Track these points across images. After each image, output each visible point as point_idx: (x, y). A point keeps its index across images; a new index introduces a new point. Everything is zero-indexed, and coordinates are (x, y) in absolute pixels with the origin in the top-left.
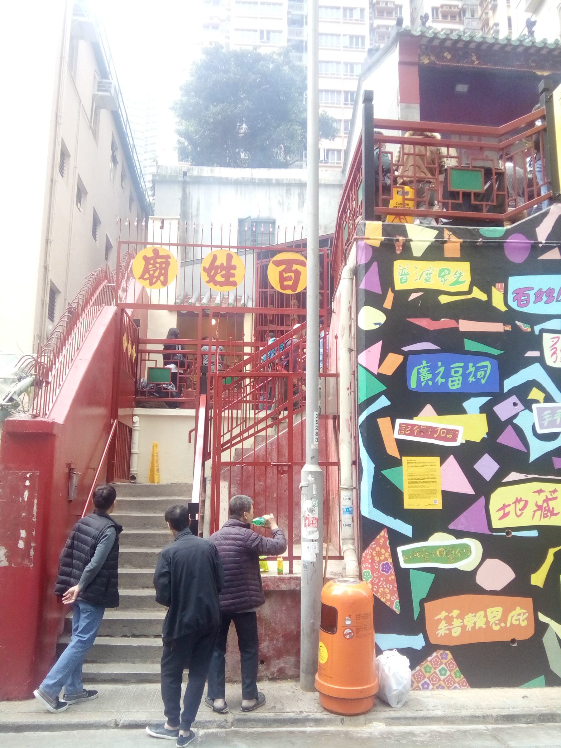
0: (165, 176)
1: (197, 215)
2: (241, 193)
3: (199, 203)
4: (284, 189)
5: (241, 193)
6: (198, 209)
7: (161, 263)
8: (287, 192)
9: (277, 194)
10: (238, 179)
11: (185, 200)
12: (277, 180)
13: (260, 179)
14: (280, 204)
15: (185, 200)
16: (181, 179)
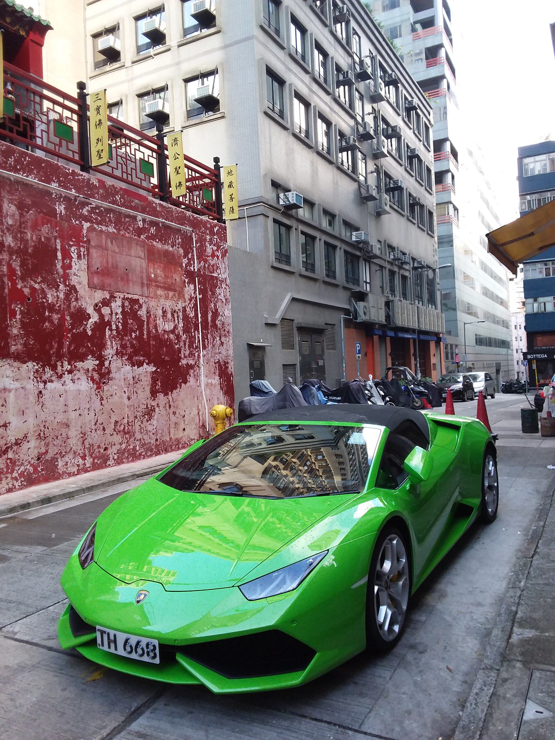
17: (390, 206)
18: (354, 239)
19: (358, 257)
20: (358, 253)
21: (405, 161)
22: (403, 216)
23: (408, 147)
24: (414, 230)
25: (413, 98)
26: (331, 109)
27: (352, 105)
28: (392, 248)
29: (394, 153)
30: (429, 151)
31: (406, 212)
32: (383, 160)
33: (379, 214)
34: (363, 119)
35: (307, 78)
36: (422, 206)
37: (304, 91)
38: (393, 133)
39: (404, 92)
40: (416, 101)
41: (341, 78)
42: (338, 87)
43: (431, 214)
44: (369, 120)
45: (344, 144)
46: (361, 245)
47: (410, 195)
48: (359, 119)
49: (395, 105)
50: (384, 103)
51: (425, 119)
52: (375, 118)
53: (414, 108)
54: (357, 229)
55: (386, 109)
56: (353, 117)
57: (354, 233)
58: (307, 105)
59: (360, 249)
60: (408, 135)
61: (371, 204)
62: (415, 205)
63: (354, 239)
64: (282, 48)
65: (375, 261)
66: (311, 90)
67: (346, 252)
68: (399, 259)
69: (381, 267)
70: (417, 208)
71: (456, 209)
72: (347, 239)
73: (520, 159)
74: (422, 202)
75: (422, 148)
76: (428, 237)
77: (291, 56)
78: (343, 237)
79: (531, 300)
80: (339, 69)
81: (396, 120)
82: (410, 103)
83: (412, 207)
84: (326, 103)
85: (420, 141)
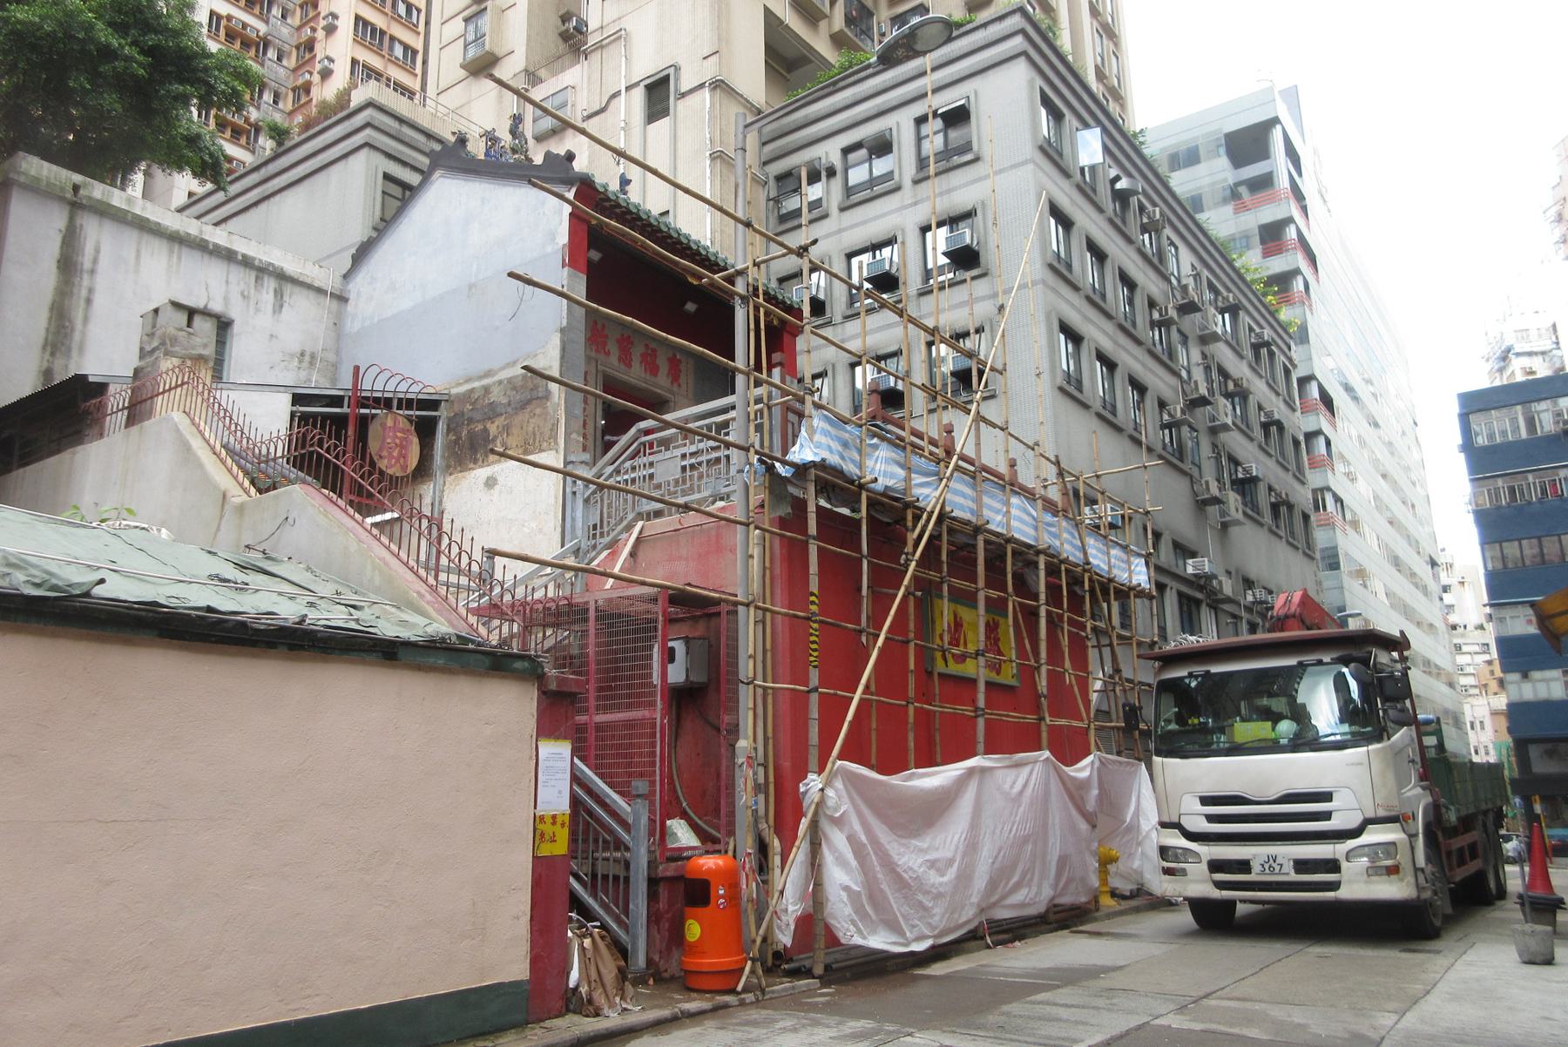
0: (38, 179)
1: (92, 272)
2: (179, 258)
3: (97, 251)
4: (253, 274)
5: (179, 258)
6: (95, 261)
7: (402, 439)
8: (257, 278)
9: (240, 279)
10: (177, 232)
11: (71, 239)
12: (244, 256)
13: (216, 245)
14: (244, 296)
15: (71, 239)
16: (69, 195)
17: (1245, 513)
18: (1190, 570)
19: (1198, 603)
20: (1199, 595)
21: (1258, 433)
22: (1261, 525)
23: (1260, 408)
24: (1281, 548)
25: (1261, 327)
26: (1143, 365)
27: (1171, 354)
28: (1249, 583)
29: (1239, 422)
30: (1294, 410)
31: (1267, 518)
32: (1223, 436)
33: (1225, 526)
34: (1189, 372)
35: (1109, 327)
36: (1290, 507)
37: (1107, 346)
38: (1240, 395)
39: (1247, 319)
40: (1267, 334)
41: (1156, 316)
42: (1152, 329)
43: (1306, 517)
44: (1198, 374)
45: (1166, 417)
46: (1202, 582)
47: (1270, 489)
48: (1184, 374)
49: (1234, 343)
50: (1221, 346)
51: (1283, 358)
52: (1207, 369)
53: (1267, 344)
54: (1193, 555)
55: (1223, 353)
56: (1176, 374)
57: (1190, 561)
58: (1110, 365)
59: (1201, 588)
60: (1259, 389)
61: (1213, 510)
62: (1281, 506)
63: (1190, 570)
64: (1076, 288)
65: (1226, 607)
66: (1116, 343)
67: (1180, 595)
68: (1261, 602)
69: (1234, 616)
70: (1283, 510)
71: (1338, 500)
72: (1179, 572)
73: (1464, 418)
74: (1292, 500)
75: (1282, 406)
76: (1306, 560)
77: (1088, 299)
78: (1174, 569)
79: (1515, 677)
80: (1152, 304)
81: (1240, 369)
82: (1259, 336)
83: (1275, 508)
84: (1136, 358)
85: (1278, 394)
